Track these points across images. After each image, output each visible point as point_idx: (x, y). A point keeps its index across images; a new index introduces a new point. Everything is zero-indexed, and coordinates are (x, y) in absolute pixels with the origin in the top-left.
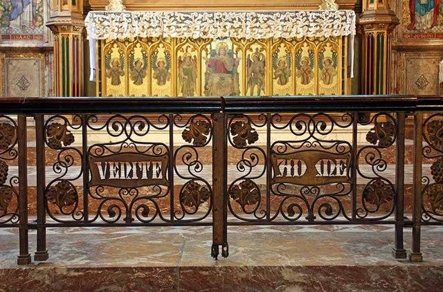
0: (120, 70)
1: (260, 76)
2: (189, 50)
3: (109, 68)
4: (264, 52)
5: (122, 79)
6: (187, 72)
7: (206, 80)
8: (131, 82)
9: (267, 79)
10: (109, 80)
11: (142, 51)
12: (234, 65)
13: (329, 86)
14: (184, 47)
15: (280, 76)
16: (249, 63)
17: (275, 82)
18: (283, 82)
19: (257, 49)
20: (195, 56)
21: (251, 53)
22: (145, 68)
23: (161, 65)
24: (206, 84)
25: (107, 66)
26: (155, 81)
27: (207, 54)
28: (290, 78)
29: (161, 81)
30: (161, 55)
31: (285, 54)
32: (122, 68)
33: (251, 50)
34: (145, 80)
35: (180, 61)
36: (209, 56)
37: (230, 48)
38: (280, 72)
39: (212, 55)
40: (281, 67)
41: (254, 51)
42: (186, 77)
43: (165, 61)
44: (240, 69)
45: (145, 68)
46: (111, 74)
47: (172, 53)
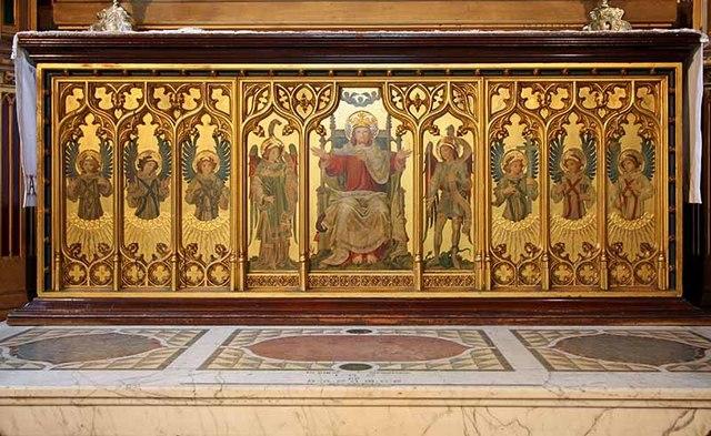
0: (101, 181)
1: (458, 197)
2: (278, 130)
3: (73, 175)
4: (468, 137)
5: (107, 203)
6: (272, 187)
7: (321, 205)
8: (130, 213)
9: (475, 205)
10: (73, 208)
11: (157, 134)
12: (393, 170)
13: (635, 225)
14: (265, 124)
15: (509, 197)
16: (429, 165)
17: (498, 212)
18: (518, 212)
19: (451, 128)
20: (292, 146)
21: (435, 140)
22: (164, 176)
23: (206, 168)
24: (322, 217)
25: (67, 171)
26: (189, 211)
27: (323, 142)
28: (535, 204)
29: (207, 210)
30: (205, 143)
31: (521, 142)
32: (106, 175)
33: (436, 131)
34: (166, 208)
35: (255, 159)
36: (328, 146)
37: (382, 126)
38: (510, 189)
39: (336, 145)
40: (512, 176)
41: (444, 133)
42: (270, 199)
43: (216, 158)
44: (408, 180)
45: (164, 176)
46: (77, 191)
47: (232, 139)
